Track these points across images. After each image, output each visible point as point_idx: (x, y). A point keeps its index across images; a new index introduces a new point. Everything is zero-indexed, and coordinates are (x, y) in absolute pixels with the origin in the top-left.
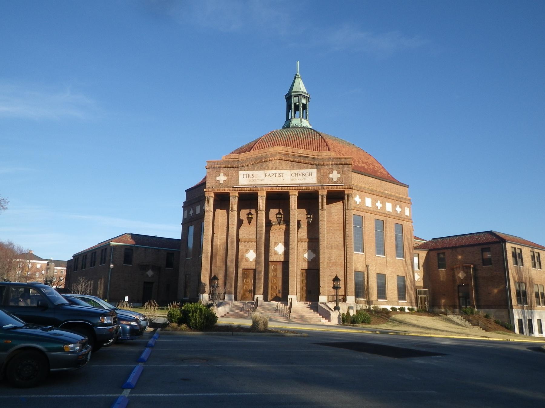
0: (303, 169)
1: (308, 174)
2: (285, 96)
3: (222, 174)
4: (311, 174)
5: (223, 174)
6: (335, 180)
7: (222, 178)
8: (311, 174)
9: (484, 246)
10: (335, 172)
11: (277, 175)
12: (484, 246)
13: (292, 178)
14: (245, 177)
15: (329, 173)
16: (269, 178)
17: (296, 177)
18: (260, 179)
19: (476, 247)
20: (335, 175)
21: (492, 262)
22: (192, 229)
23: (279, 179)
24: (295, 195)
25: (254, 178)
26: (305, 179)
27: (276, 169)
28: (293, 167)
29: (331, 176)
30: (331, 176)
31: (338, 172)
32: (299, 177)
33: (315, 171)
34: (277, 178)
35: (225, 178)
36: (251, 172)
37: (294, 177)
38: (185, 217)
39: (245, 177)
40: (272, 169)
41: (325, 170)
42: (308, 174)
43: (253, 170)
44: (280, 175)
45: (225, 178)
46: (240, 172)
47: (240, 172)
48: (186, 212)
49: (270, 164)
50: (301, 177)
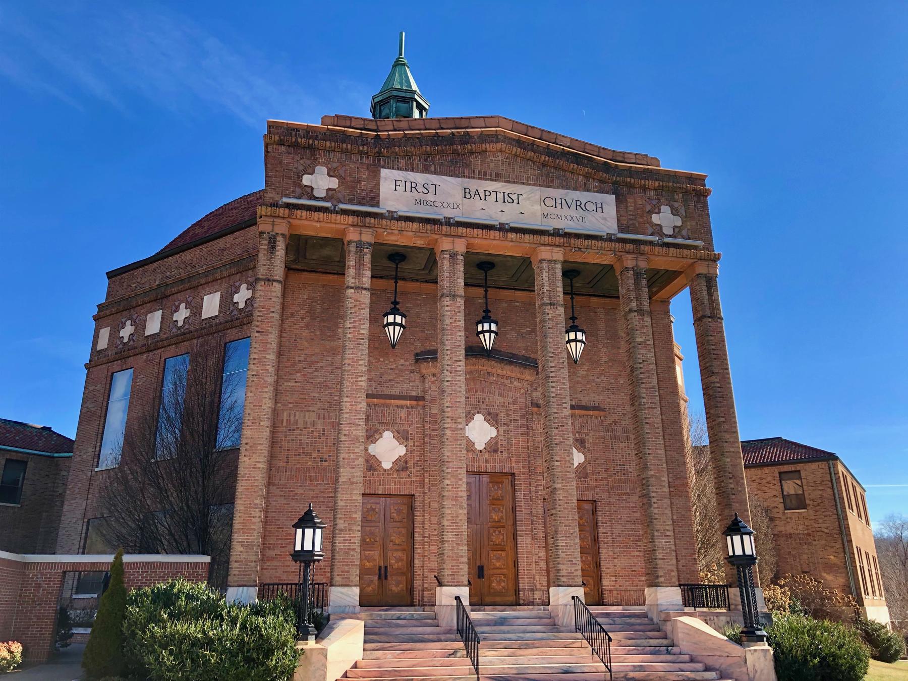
0: (576, 189)
1: (591, 207)
2: (374, 98)
3: (321, 170)
4: (599, 208)
5: (325, 170)
6: (668, 231)
7: (321, 181)
8: (599, 208)
9: (786, 468)
10: (665, 209)
11: (500, 196)
12: (786, 468)
13: (547, 211)
14: (400, 189)
15: (650, 212)
16: (479, 204)
17: (558, 211)
18: (450, 200)
19: (766, 470)
20: (665, 219)
21: (808, 502)
22: (122, 383)
23: (507, 207)
24: (555, 262)
25: (430, 197)
26: (584, 219)
27: (497, 177)
28: (547, 181)
29: (655, 219)
30: (655, 219)
31: (675, 212)
32: (565, 211)
33: (610, 200)
34: (500, 206)
35: (334, 183)
36: (419, 178)
37: (553, 210)
38: (103, 344)
39: (400, 189)
40: (483, 176)
41: (639, 202)
42: (591, 207)
43: (426, 170)
44: (508, 199)
45: (334, 183)
46: (384, 172)
47: (384, 172)
48: (105, 333)
49: (476, 162)
50: (572, 212)
